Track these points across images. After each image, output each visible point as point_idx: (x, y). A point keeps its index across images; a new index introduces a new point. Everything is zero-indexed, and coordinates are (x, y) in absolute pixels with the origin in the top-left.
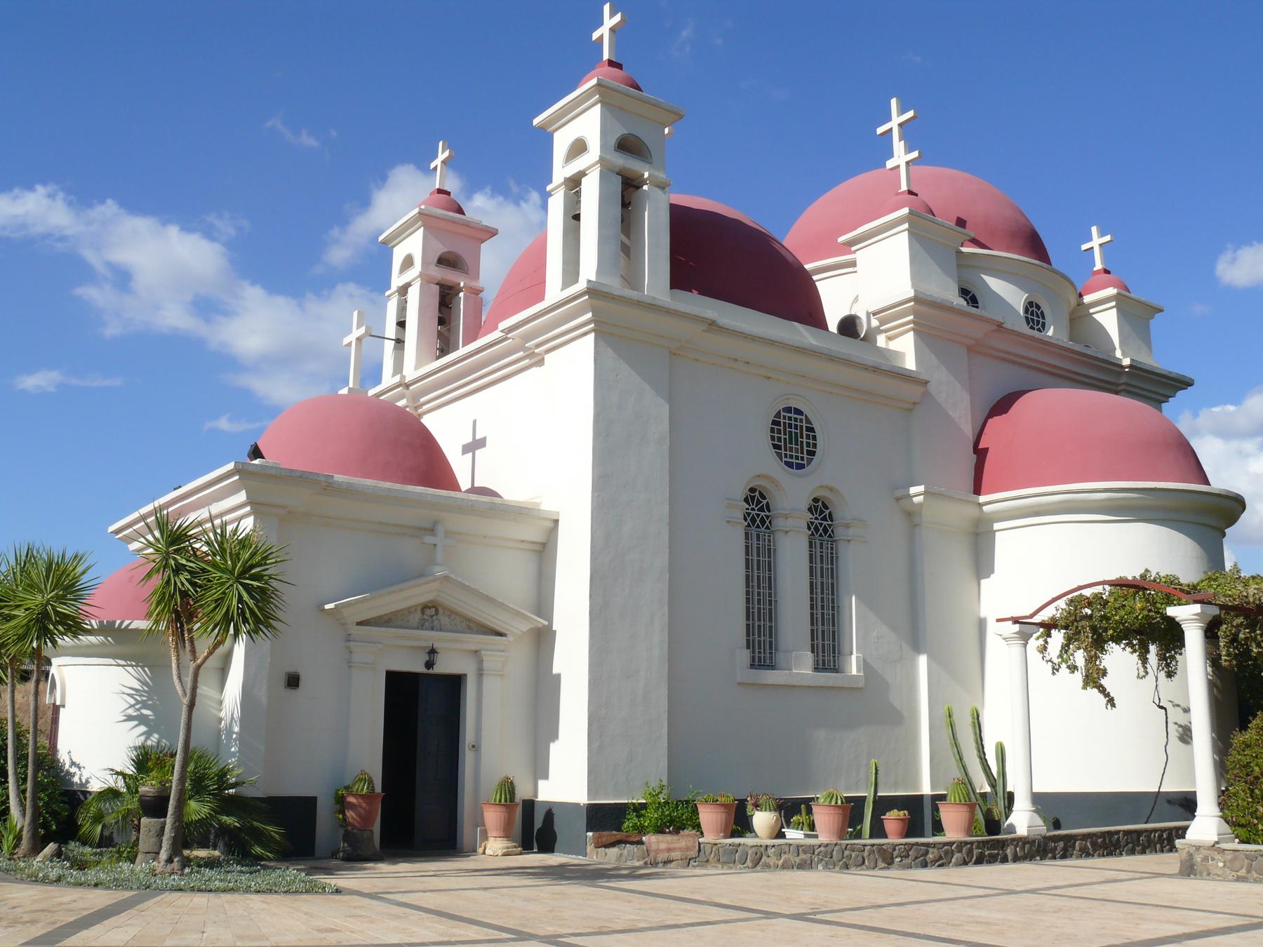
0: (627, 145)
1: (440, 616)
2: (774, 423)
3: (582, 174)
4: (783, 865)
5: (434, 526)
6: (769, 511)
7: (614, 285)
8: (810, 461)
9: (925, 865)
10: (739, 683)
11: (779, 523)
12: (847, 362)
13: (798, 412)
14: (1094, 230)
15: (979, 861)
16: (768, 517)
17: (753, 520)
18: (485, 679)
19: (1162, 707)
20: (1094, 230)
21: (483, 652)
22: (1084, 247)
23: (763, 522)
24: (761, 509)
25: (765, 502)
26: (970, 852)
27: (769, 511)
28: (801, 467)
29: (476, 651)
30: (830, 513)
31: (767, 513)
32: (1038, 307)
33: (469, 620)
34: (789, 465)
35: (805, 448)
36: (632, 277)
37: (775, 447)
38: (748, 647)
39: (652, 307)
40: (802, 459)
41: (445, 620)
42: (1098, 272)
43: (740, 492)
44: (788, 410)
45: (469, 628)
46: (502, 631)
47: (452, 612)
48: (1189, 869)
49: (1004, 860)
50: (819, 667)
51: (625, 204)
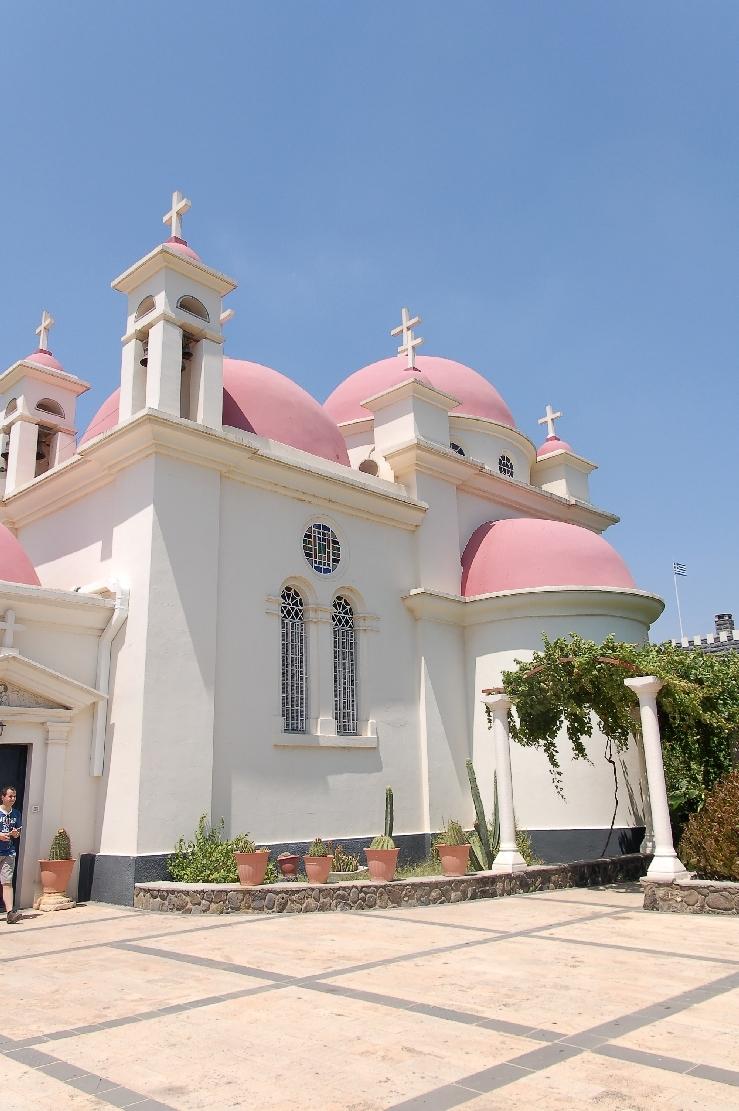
0: (187, 305)
1: (9, 693)
2: (306, 536)
3: (151, 325)
4: (306, 908)
5: (5, 613)
6: (302, 605)
7: (174, 412)
8: (334, 568)
9: (426, 904)
10: (275, 746)
11: (312, 615)
12: (363, 490)
13: (325, 528)
14: (548, 409)
15: (473, 897)
16: (301, 611)
17: (289, 613)
18: (50, 747)
19: (610, 762)
20: (548, 409)
21: (48, 724)
22: (540, 421)
23: (297, 614)
24: (296, 604)
25: (292, 592)
26: (464, 893)
27: (302, 605)
28: (327, 571)
29: (43, 723)
30: (350, 609)
31: (300, 608)
32: (508, 460)
33: (36, 696)
34: (318, 569)
35: (332, 557)
36: (187, 409)
37: (307, 555)
38: (283, 715)
39: (206, 434)
40: (329, 565)
41: (12, 696)
42: (551, 439)
43: (279, 590)
44: (318, 527)
45: (37, 703)
46: (68, 705)
47: (19, 690)
48: (652, 905)
49: (493, 895)
50: (343, 730)
51: (187, 355)
